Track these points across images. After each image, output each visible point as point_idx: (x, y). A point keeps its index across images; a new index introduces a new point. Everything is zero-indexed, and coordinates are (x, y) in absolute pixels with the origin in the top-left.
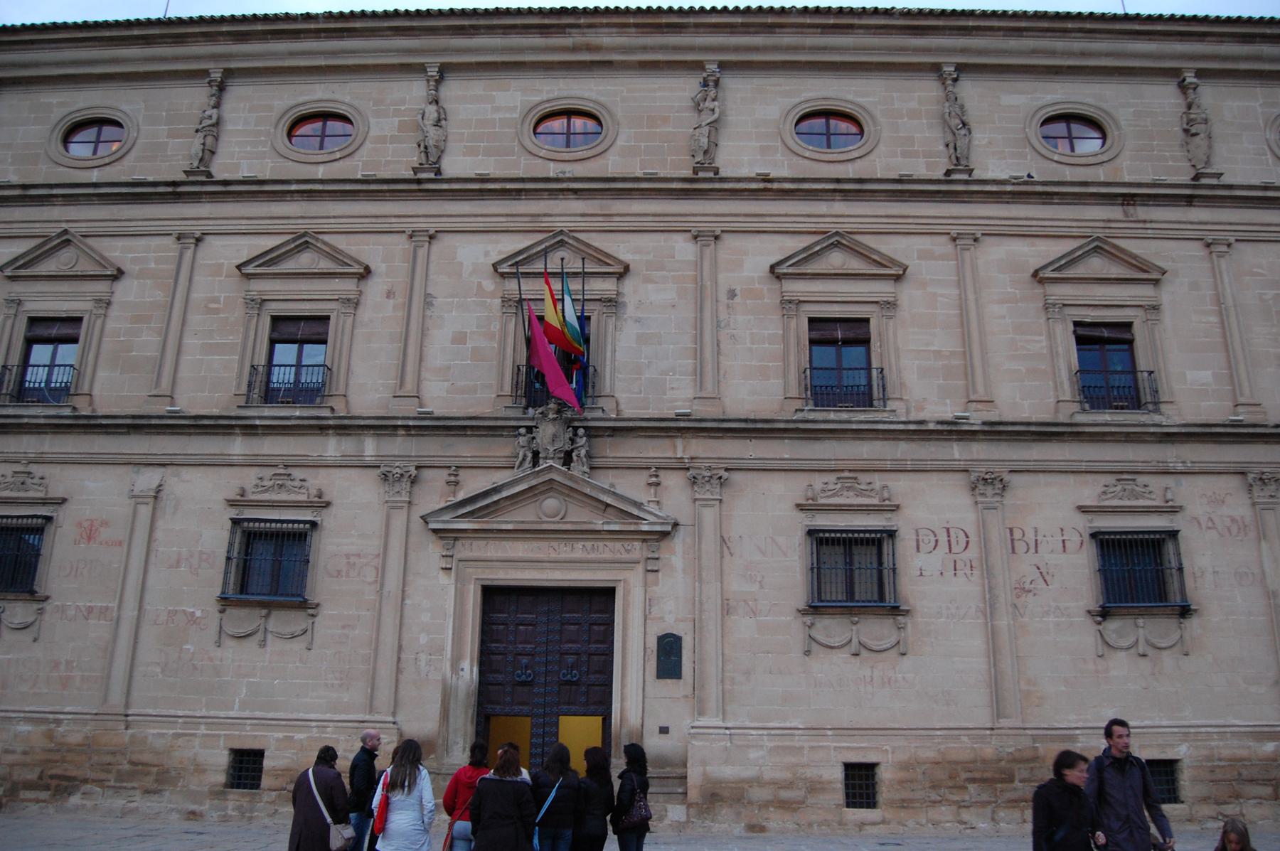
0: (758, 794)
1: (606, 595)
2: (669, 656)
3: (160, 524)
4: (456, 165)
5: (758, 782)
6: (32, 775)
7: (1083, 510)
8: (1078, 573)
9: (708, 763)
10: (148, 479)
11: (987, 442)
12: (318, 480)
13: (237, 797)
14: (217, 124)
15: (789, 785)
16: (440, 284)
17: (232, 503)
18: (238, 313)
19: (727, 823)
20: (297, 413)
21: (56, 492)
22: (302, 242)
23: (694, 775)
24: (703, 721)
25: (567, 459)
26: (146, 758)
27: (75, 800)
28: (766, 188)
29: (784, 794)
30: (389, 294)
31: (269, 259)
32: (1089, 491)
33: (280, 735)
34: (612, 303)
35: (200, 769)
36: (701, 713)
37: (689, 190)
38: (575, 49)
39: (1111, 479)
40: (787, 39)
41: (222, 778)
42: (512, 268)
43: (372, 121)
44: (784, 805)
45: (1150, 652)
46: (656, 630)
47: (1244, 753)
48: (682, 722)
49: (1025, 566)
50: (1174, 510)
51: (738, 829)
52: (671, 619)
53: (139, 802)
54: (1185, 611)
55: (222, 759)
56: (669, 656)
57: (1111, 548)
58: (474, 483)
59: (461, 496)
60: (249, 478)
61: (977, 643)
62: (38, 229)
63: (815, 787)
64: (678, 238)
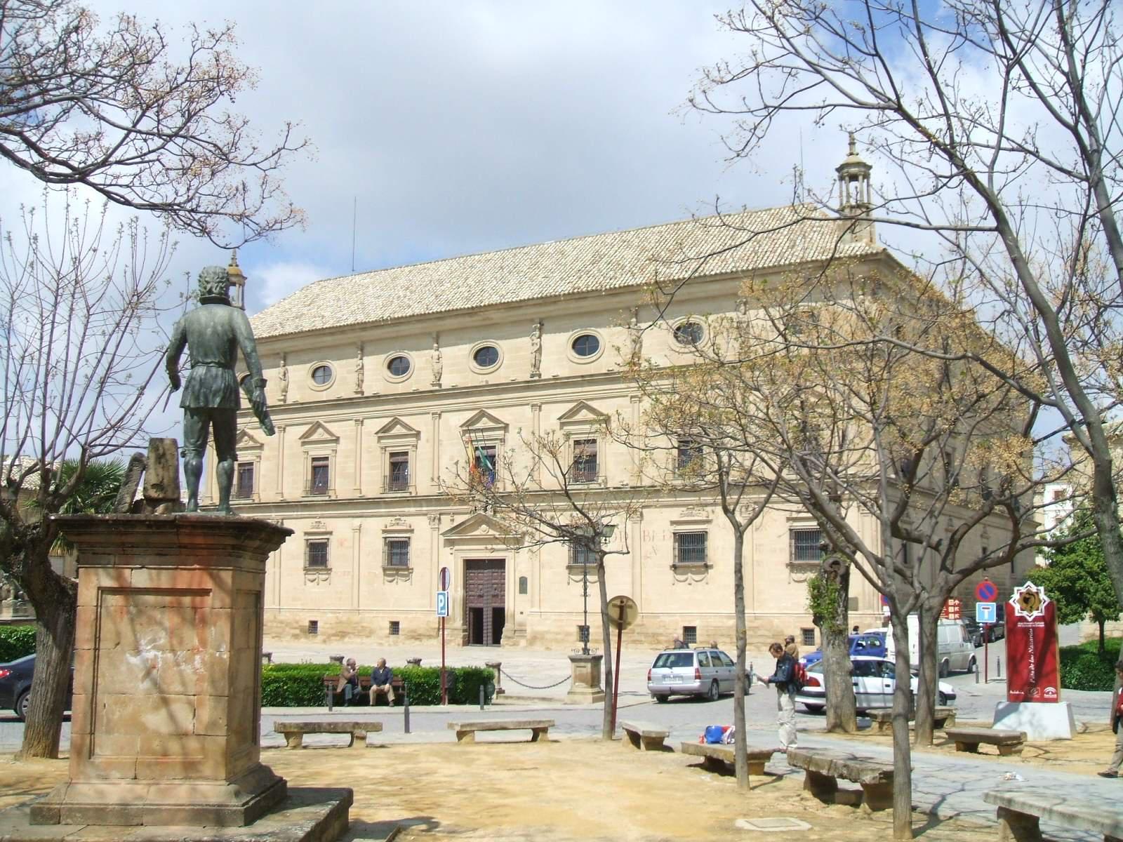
0: (548, 636)
1: (500, 564)
2: (523, 583)
3: (363, 539)
4: (447, 382)
5: (547, 632)
6: (334, 632)
7: (673, 523)
8: (667, 550)
9: (534, 625)
10: (357, 522)
11: (635, 496)
12: (409, 520)
13: (393, 637)
14: (362, 368)
15: (558, 634)
16: (443, 435)
17: (384, 531)
18: (378, 452)
19: (538, 647)
20: (399, 495)
21: (328, 530)
22: (396, 422)
23: (529, 630)
24: (533, 610)
25: (486, 510)
26: (364, 624)
27: (346, 639)
28: (557, 383)
29: (559, 637)
30: (427, 441)
31: (385, 429)
32: (676, 514)
33: (404, 616)
34: (503, 441)
35: (381, 629)
36: (532, 607)
37: (528, 386)
38: (484, 320)
39: (684, 509)
40: (561, 306)
41: (388, 631)
42: (468, 427)
43: (416, 360)
44: (557, 641)
45: (693, 582)
46: (518, 576)
47: (720, 624)
48: (527, 610)
49: (647, 547)
50: (708, 522)
51: (543, 649)
52: (523, 570)
53: (365, 640)
54: (707, 567)
55: (388, 625)
56: (523, 583)
57: (681, 538)
58: (459, 519)
59: (455, 524)
60: (388, 520)
61: (629, 579)
62: (309, 420)
63: (568, 634)
64: (528, 408)
